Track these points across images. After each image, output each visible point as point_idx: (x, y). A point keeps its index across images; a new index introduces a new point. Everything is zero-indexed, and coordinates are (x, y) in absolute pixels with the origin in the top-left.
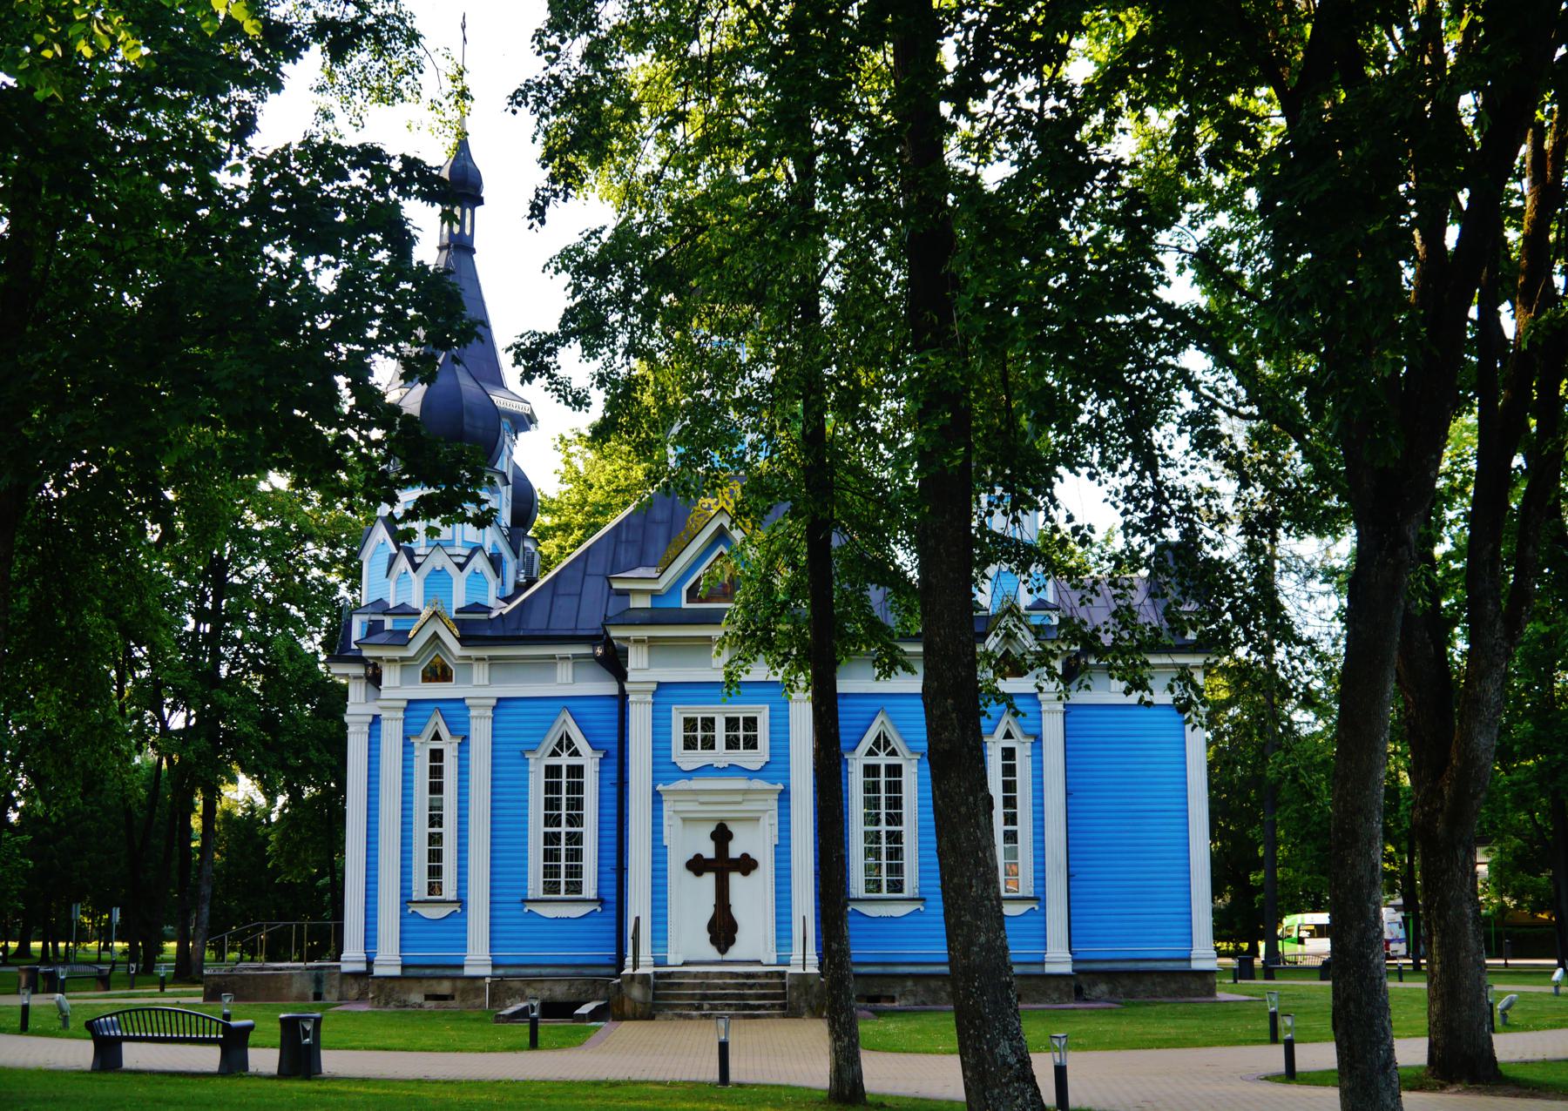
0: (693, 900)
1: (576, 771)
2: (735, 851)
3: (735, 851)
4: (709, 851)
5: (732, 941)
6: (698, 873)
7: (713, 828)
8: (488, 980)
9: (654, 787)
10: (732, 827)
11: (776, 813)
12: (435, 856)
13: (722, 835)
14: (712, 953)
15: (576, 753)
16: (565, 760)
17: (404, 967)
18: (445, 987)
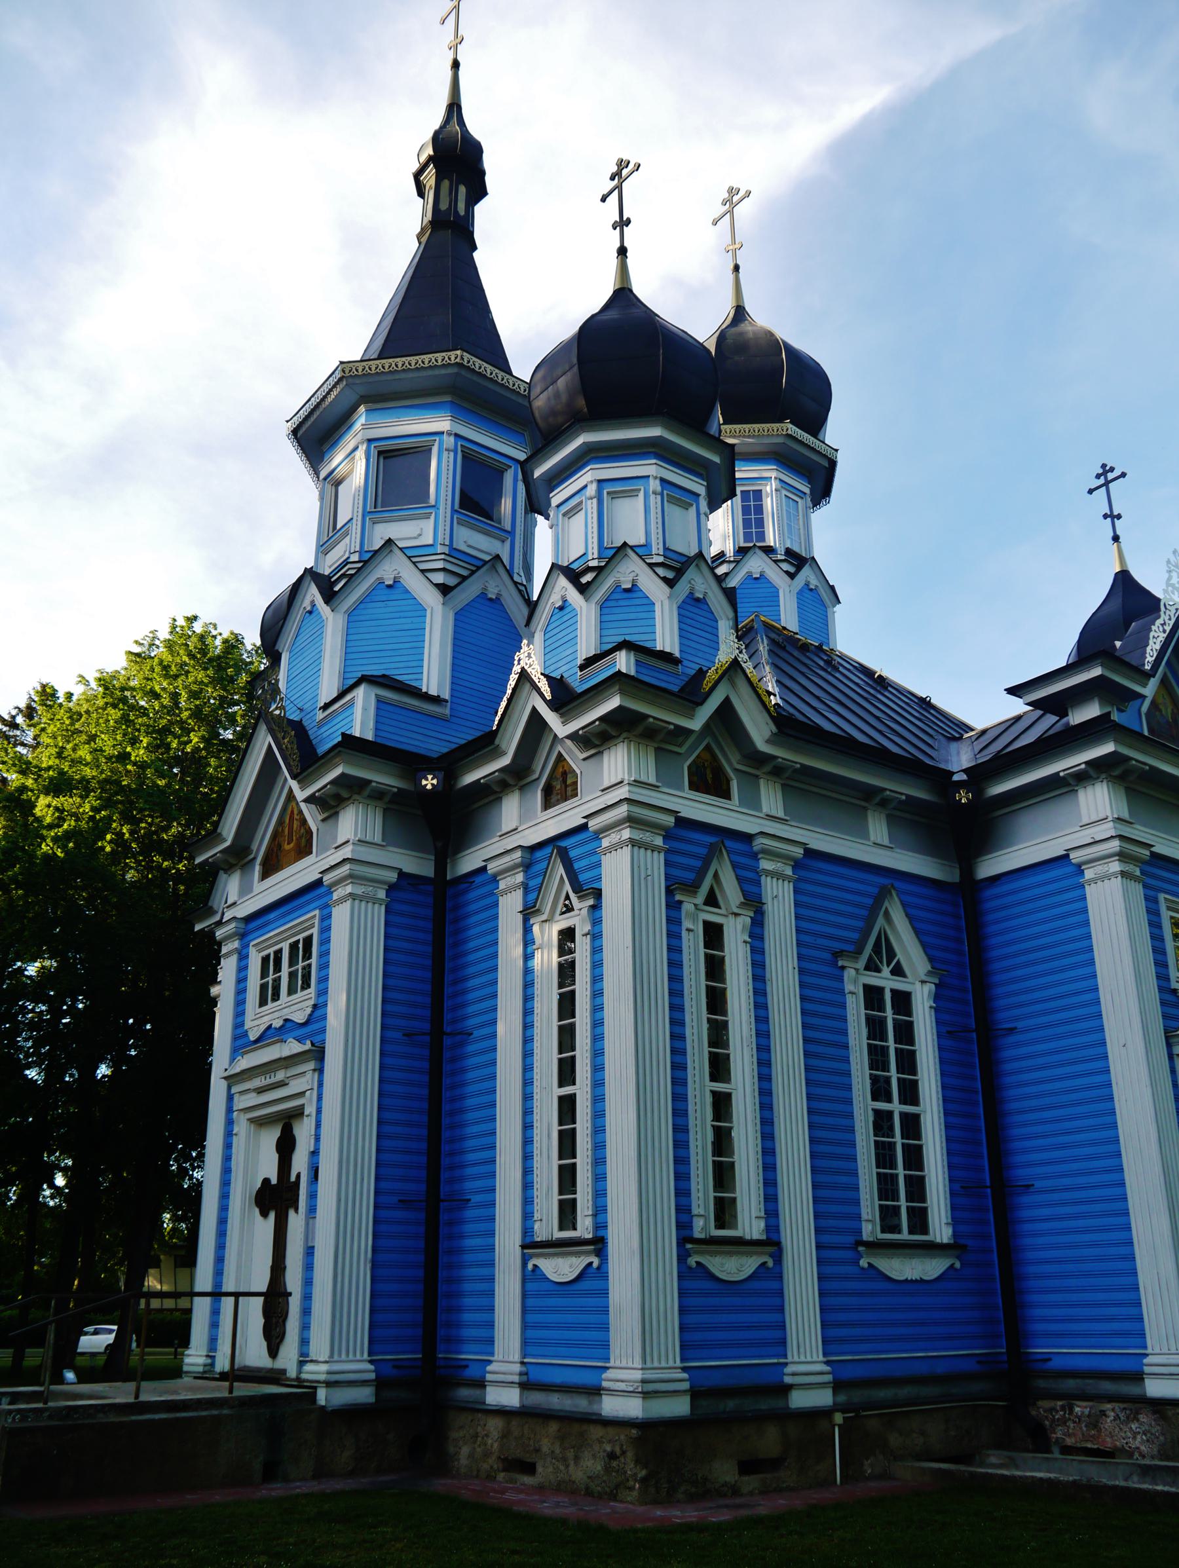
1: (903, 1001)
8: (838, 1418)
12: (722, 1141)
15: (898, 971)
16: (885, 980)
17: (695, 1394)
18: (769, 1441)
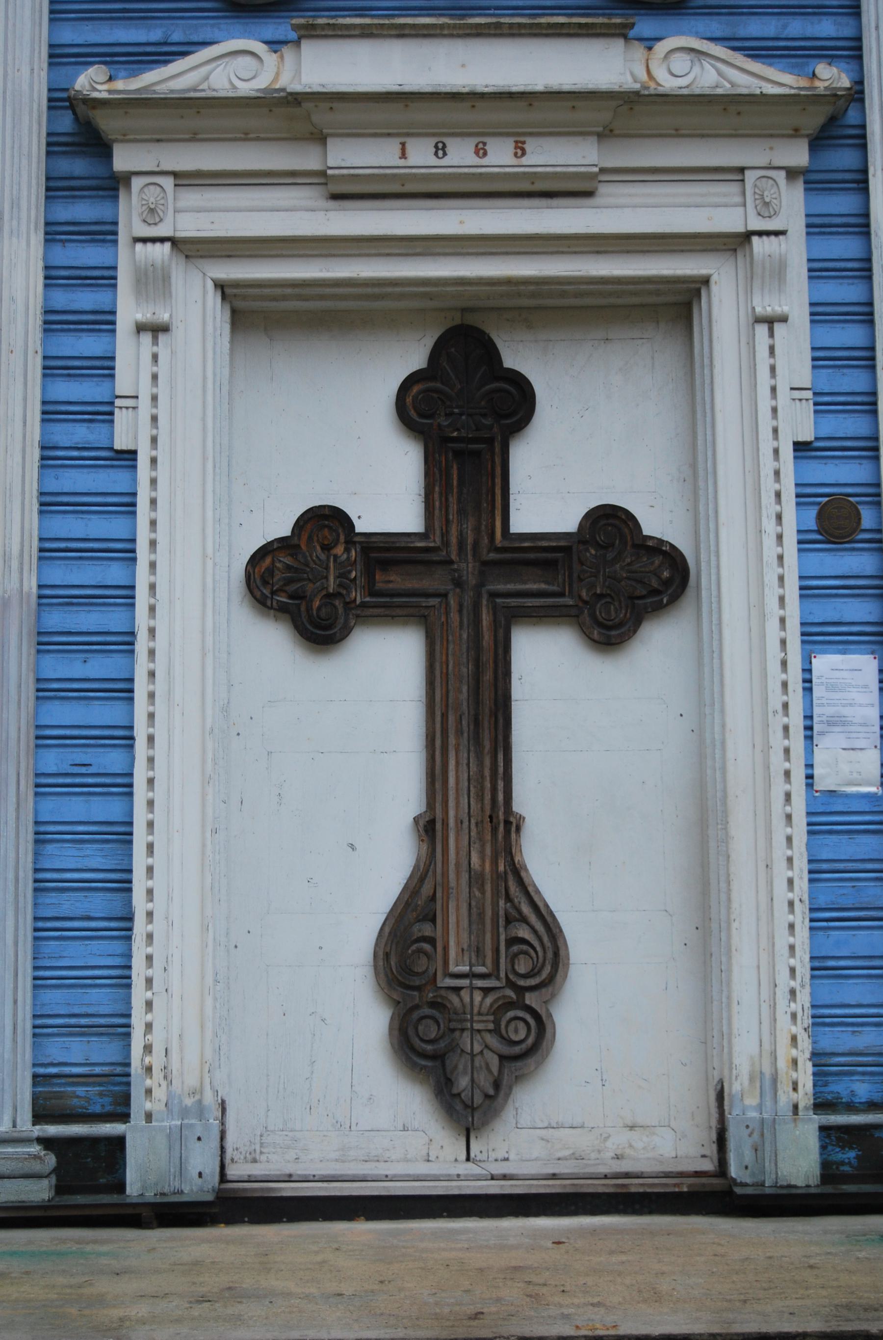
0: (278, 800)
2: (548, 490)
3: (548, 490)
4: (388, 494)
5: (526, 1042)
6: (321, 630)
7: (410, 356)
9: (61, 100)
10: (517, 356)
11: (795, 250)
13: (466, 409)
14: (388, 1128)
